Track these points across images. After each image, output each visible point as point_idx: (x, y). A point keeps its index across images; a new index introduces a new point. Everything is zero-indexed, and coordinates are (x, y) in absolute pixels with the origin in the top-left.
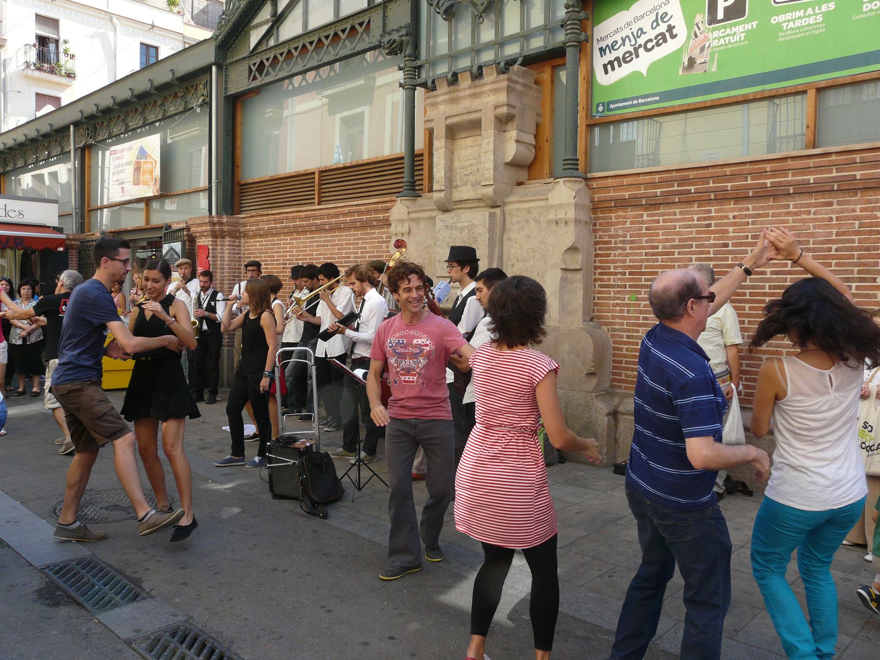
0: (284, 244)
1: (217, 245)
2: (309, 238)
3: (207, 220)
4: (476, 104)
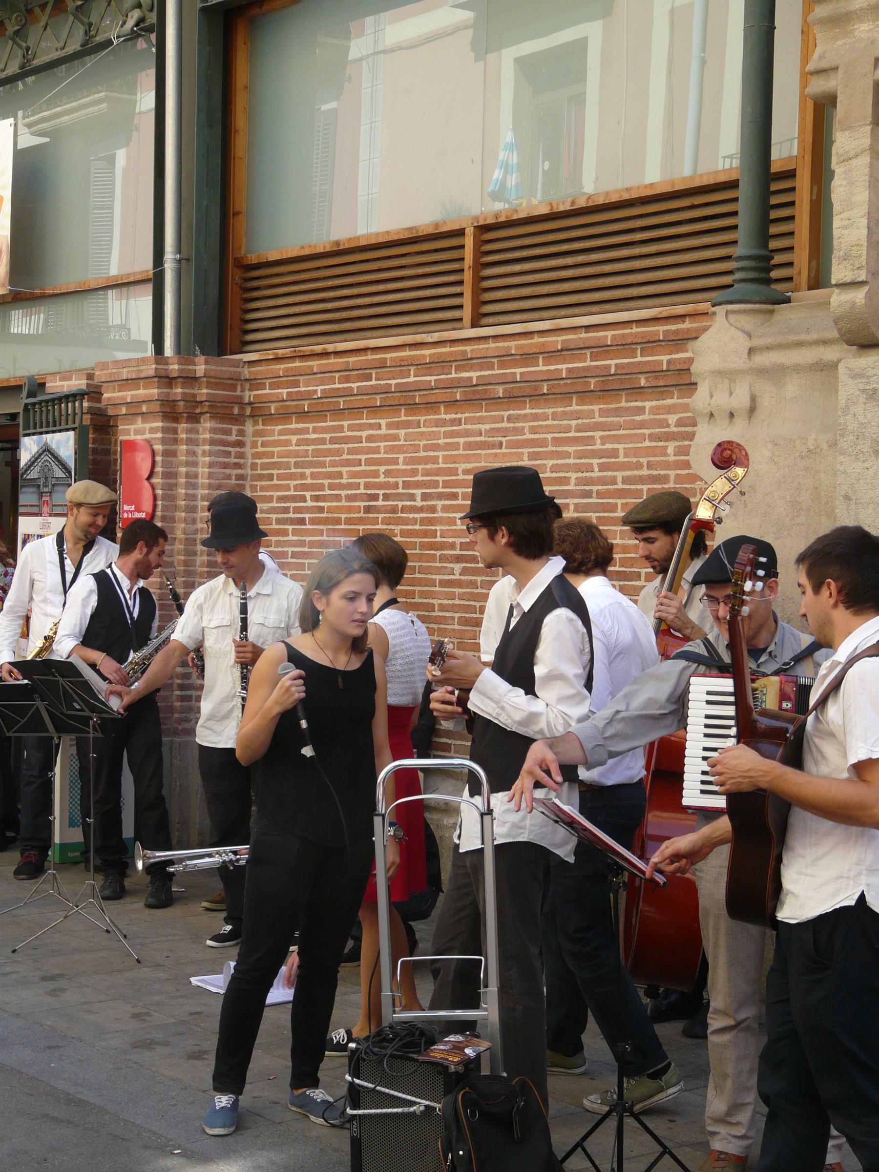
0: (369, 439)
1: (175, 441)
2: (444, 423)
3: (150, 369)
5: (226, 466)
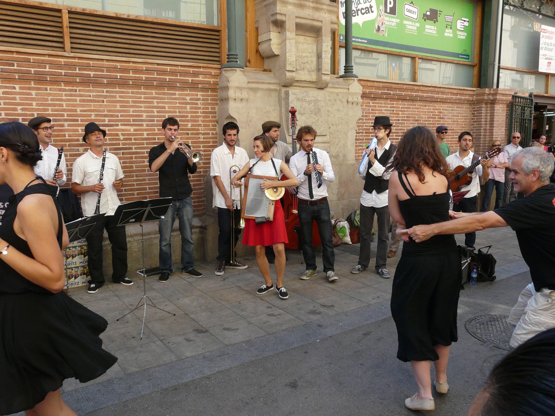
2: (65, 90)
4: (317, 15)
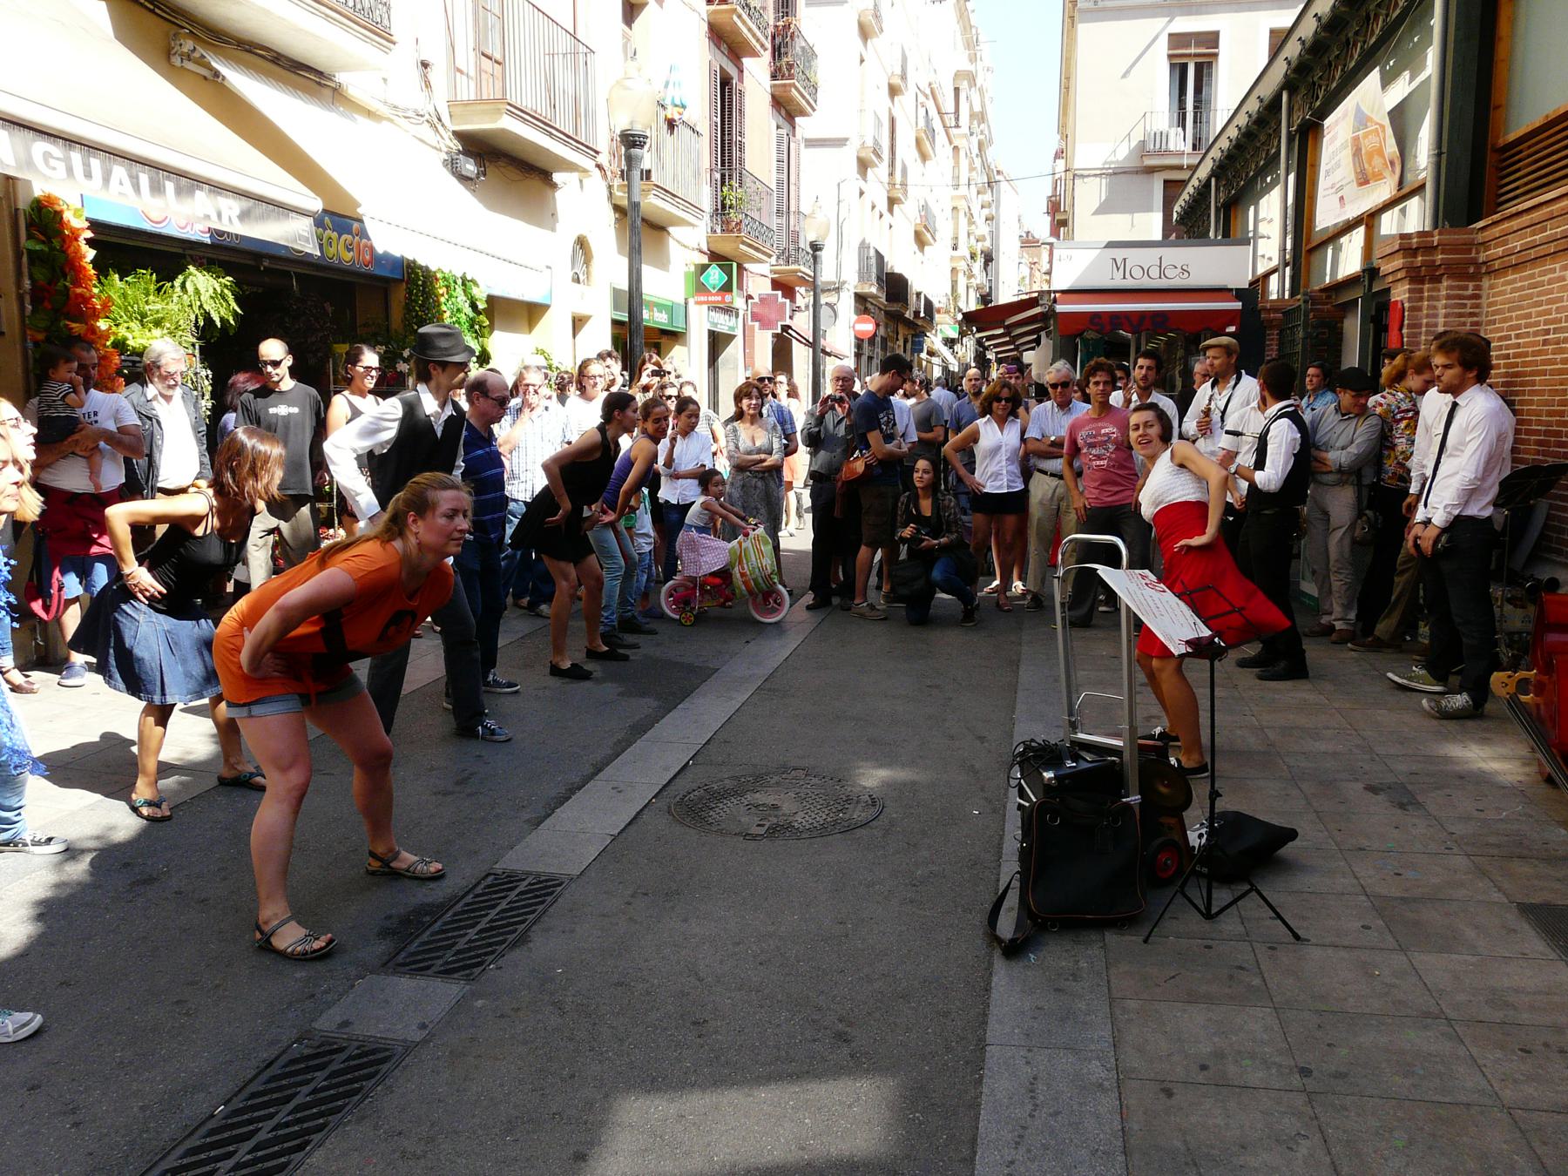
1: (1421, 299)
5: (1461, 315)
